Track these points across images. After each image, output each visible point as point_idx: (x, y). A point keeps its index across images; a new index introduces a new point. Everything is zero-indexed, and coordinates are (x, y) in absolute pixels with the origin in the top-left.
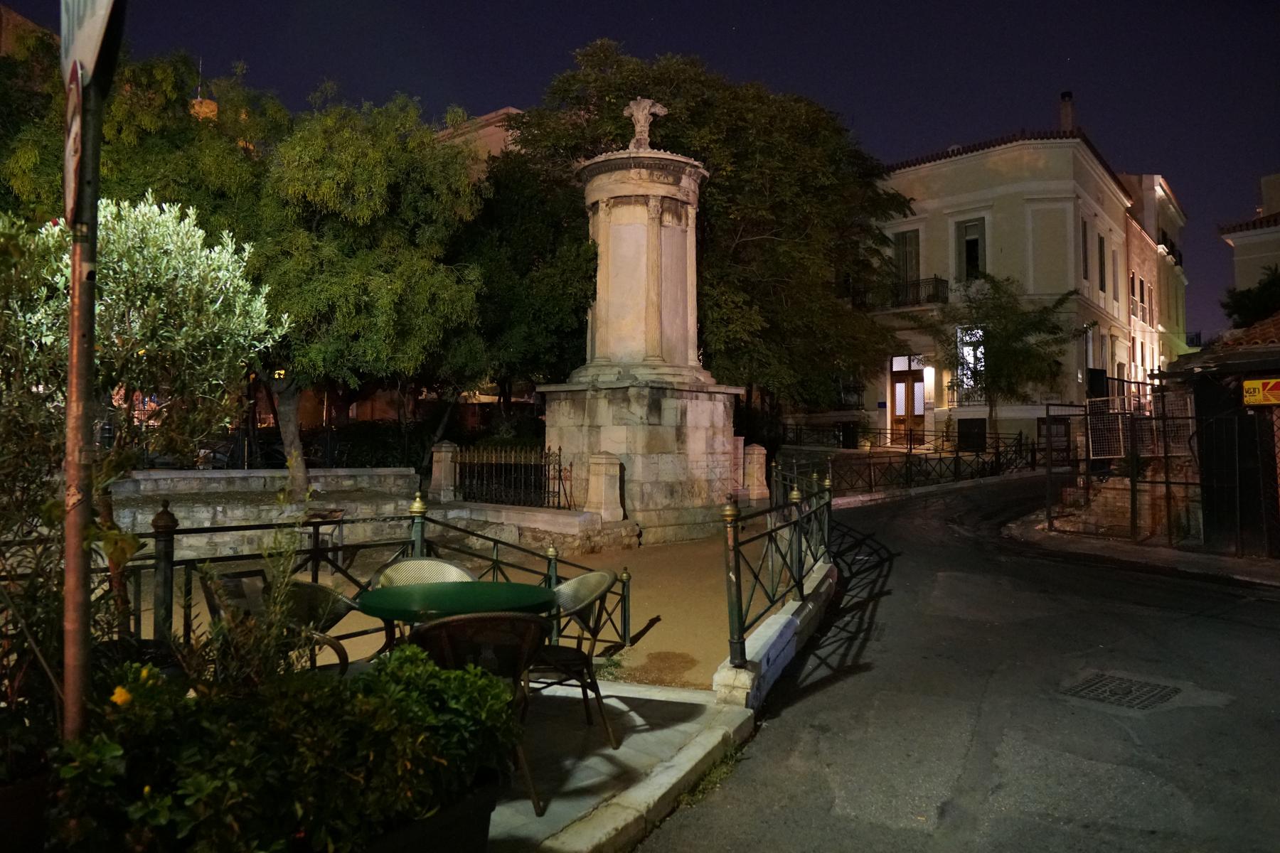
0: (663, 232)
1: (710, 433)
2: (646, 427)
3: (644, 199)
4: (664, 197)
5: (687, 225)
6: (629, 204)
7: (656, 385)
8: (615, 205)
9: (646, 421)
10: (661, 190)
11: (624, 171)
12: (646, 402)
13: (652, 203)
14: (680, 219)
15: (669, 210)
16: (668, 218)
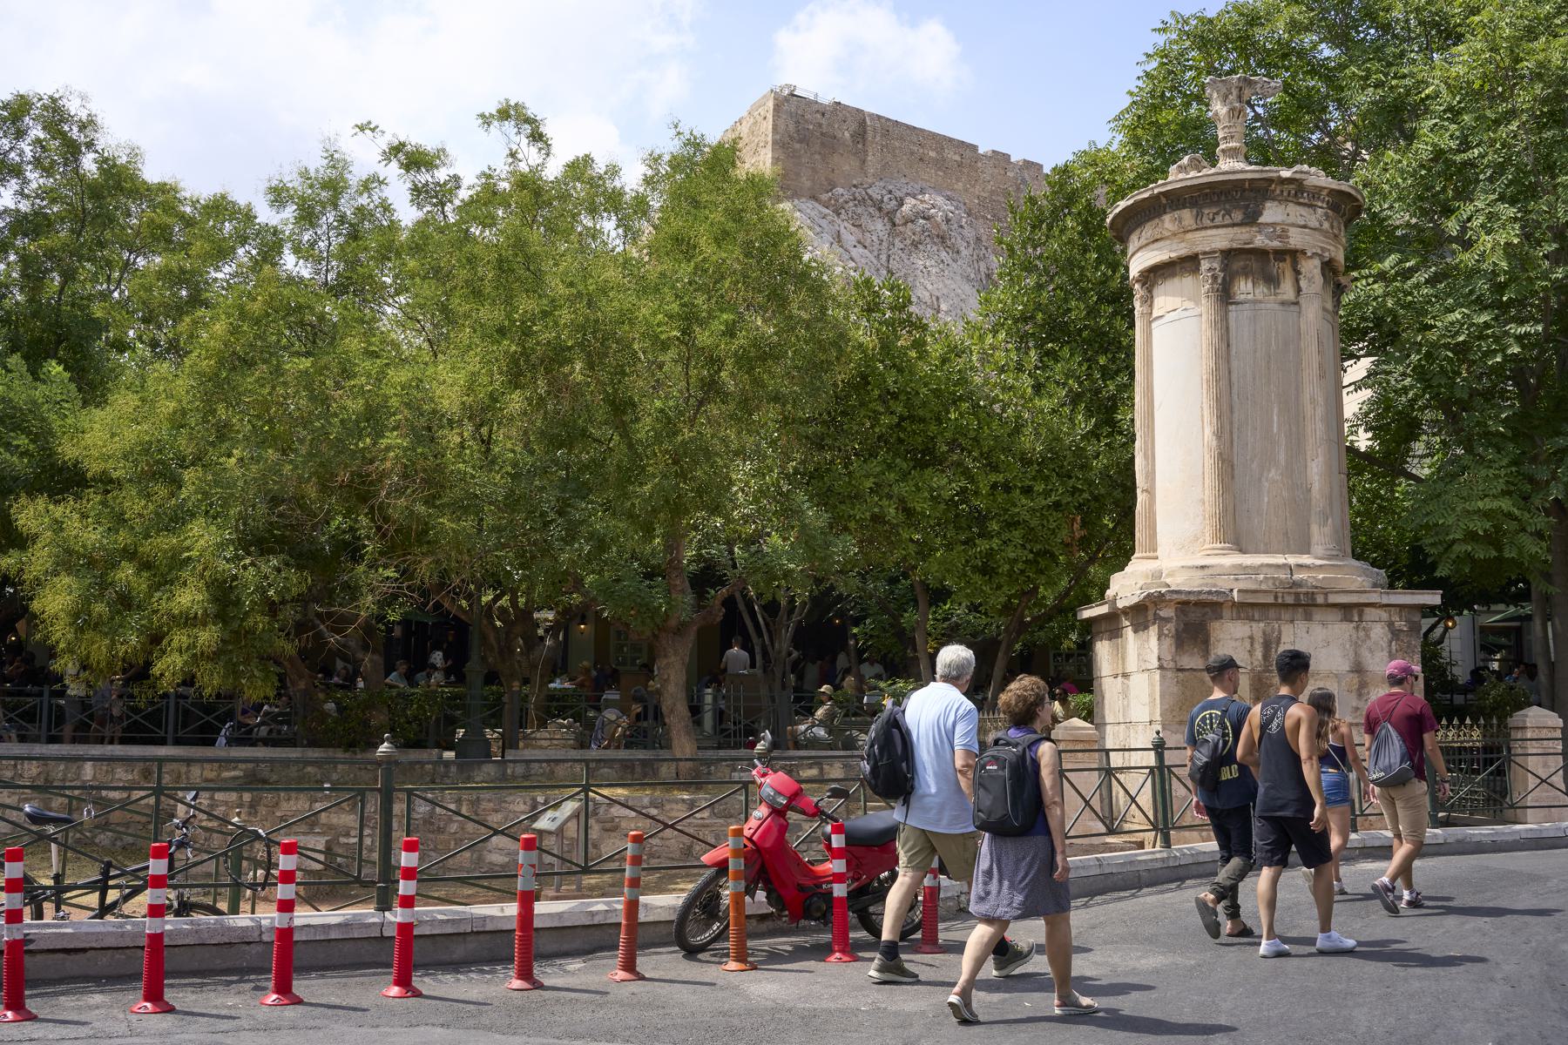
0: (1232, 316)
1: (1355, 679)
2: (1169, 674)
3: (1187, 264)
4: (1228, 255)
5: (1299, 290)
6: (1173, 275)
7: (1183, 597)
8: (1152, 286)
9: (1172, 665)
10: (1220, 239)
11: (1157, 220)
12: (1170, 628)
13: (1205, 265)
14: (1272, 281)
15: (1246, 273)
16: (1244, 288)
